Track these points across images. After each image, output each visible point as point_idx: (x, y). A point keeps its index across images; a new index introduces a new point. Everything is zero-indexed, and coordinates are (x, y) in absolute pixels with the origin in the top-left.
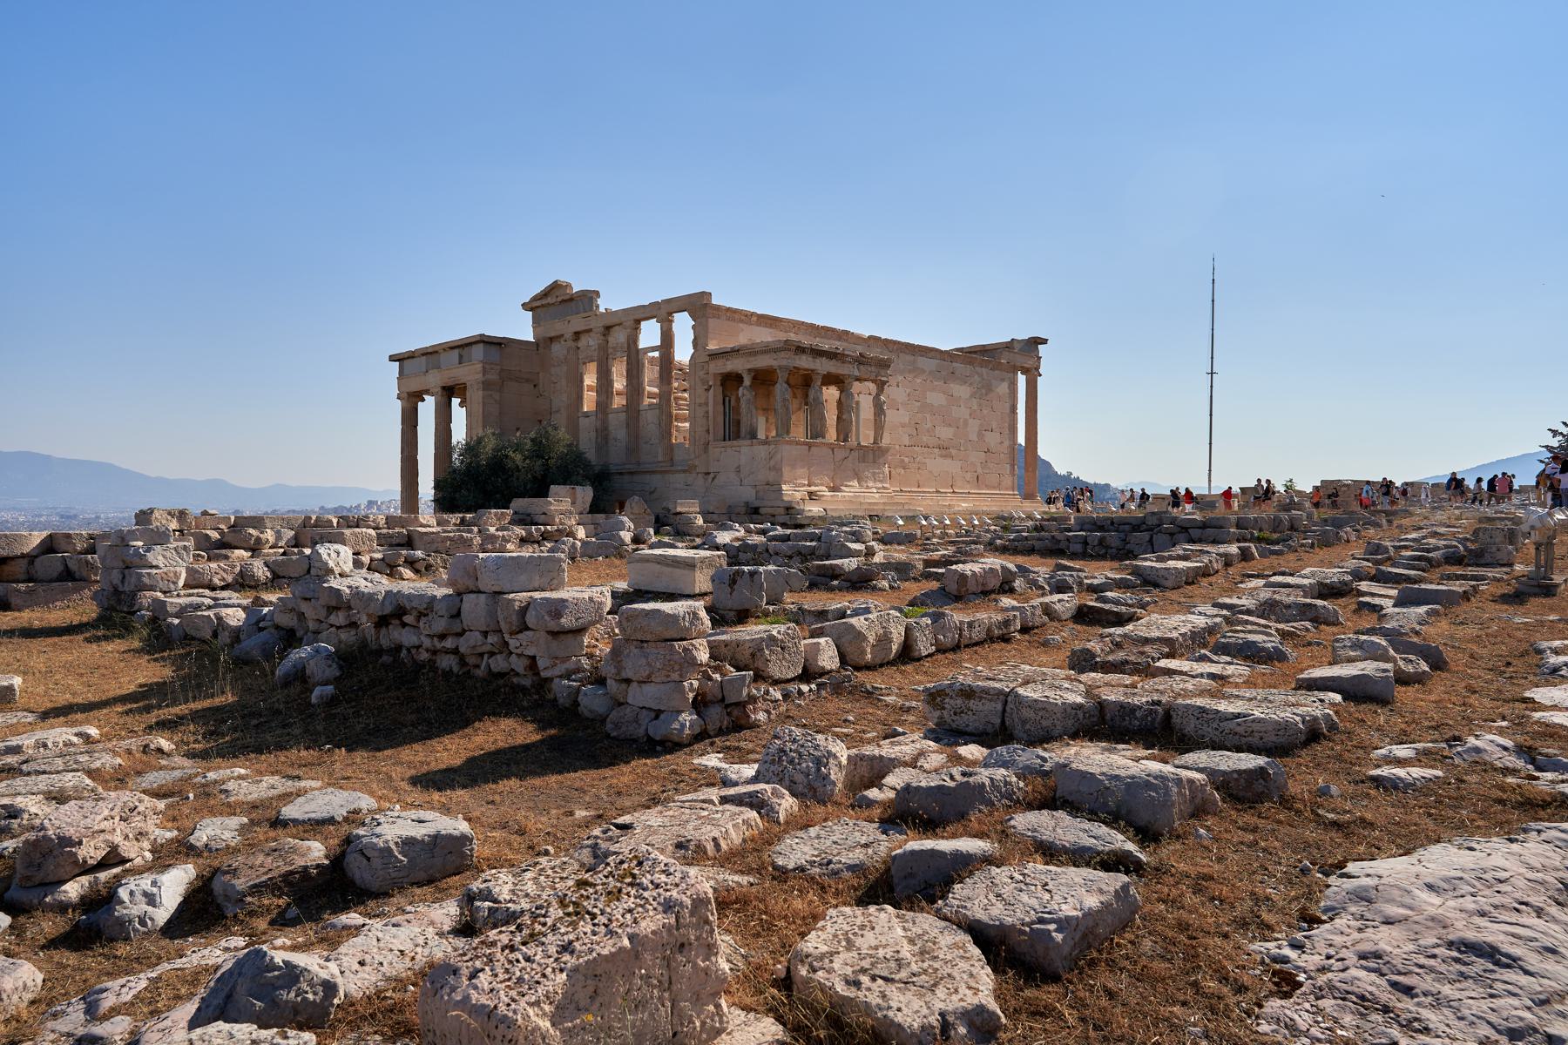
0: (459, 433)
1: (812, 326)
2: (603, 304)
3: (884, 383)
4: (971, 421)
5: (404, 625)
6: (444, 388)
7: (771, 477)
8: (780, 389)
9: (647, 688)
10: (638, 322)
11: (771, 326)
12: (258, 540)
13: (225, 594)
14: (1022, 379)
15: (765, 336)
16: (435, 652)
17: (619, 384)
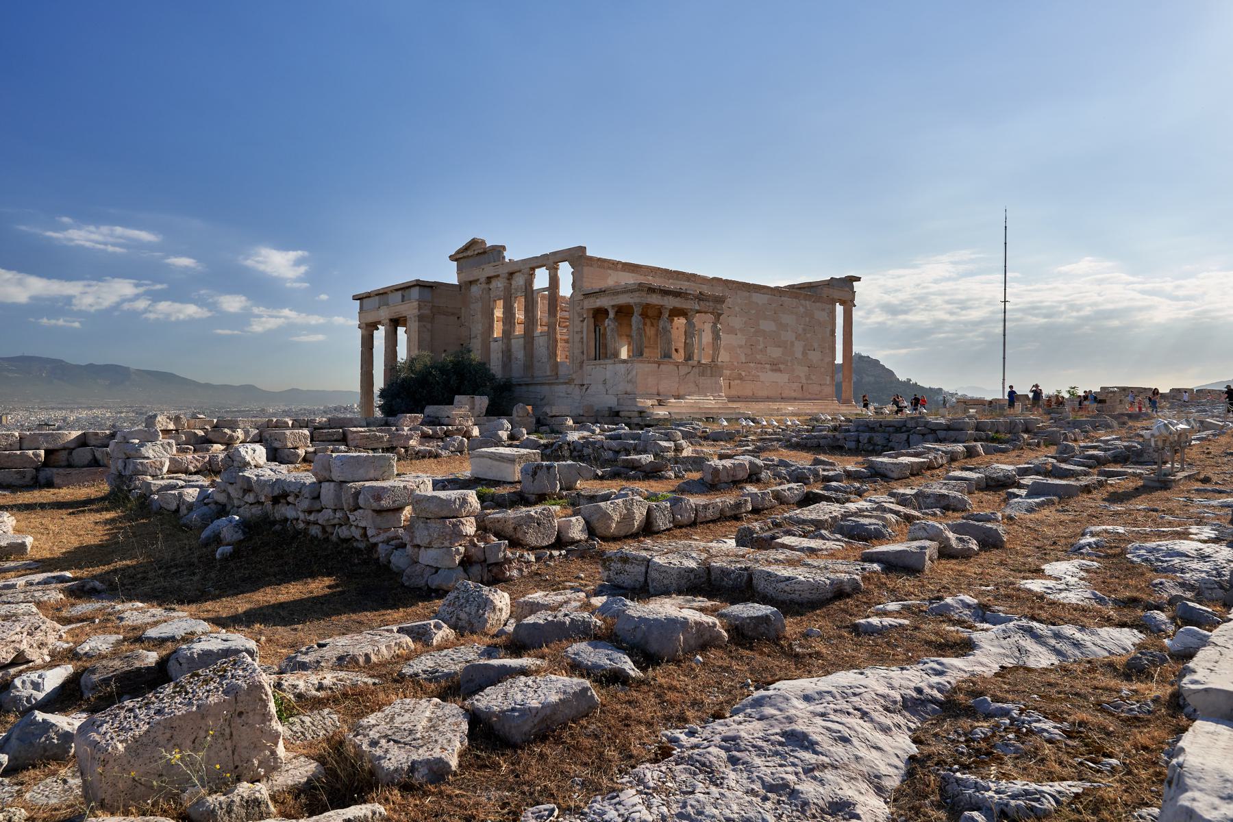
0: (402, 354)
1: (666, 271)
2: (509, 255)
3: (720, 315)
4: (796, 343)
5: (288, 504)
6: (391, 320)
7: (629, 388)
8: (636, 319)
9: (431, 552)
10: (533, 269)
11: (633, 272)
12: (231, 437)
13: (195, 477)
14: (839, 309)
15: (629, 279)
16: (308, 523)
17: (520, 315)
